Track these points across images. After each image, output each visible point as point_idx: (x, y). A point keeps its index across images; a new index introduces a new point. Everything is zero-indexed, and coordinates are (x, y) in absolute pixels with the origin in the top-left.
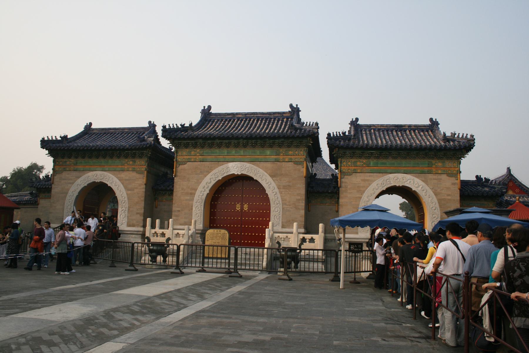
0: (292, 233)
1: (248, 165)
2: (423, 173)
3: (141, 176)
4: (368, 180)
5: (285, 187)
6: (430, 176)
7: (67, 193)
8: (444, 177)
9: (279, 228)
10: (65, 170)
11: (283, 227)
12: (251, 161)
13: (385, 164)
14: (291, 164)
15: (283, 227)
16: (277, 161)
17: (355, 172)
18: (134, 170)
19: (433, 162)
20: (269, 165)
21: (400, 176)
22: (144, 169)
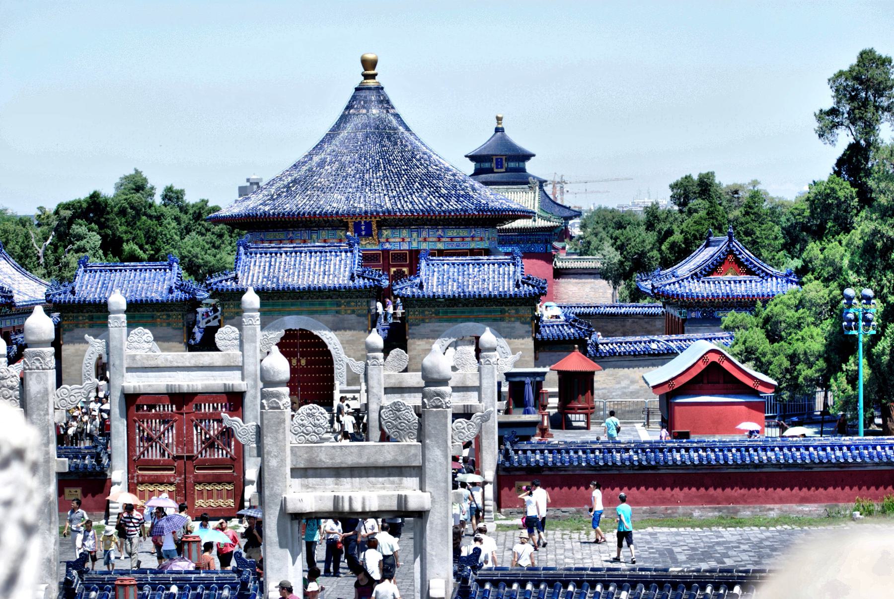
0: (358, 391)
1: (304, 318)
2: (495, 320)
3: (178, 332)
4: (437, 331)
5: (348, 342)
6: (503, 324)
7: (83, 356)
8: (518, 325)
9: (345, 388)
10: (77, 326)
11: (348, 384)
12: (311, 313)
13: (455, 312)
14: (353, 317)
15: (348, 384)
16: (338, 312)
17: (423, 321)
18: (169, 325)
19: (507, 309)
20: (329, 318)
21: (471, 324)
22: (180, 325)
